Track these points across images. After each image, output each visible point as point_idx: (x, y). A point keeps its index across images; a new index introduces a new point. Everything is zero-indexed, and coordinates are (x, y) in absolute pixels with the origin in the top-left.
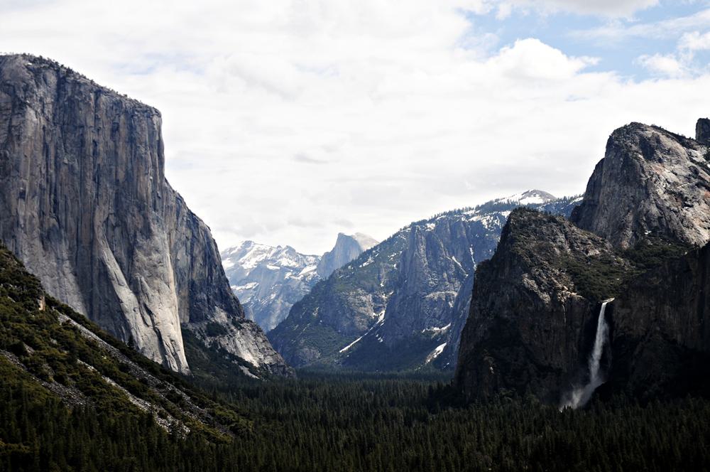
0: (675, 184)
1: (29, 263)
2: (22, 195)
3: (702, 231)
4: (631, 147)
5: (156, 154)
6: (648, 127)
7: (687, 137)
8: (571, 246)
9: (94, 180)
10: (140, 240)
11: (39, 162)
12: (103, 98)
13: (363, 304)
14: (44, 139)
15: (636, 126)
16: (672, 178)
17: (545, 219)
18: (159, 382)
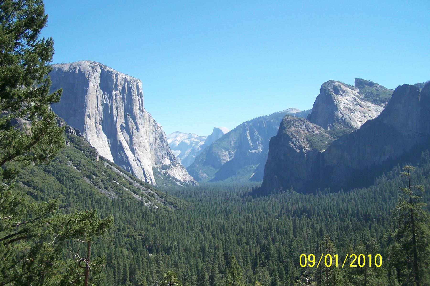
0: (347, 104)
1: (92, 143)
2: (89, 117)
3: (358, 123)
5: (140, 98)
7: (352, 85)
8: (308, 130)
10: (135, 132)
11: (95, 103)
12: (119, 76)
13: (225, 155)
14: (96, 94)
15: (332, 82)
16: (346, 102)
18: (145, 189)
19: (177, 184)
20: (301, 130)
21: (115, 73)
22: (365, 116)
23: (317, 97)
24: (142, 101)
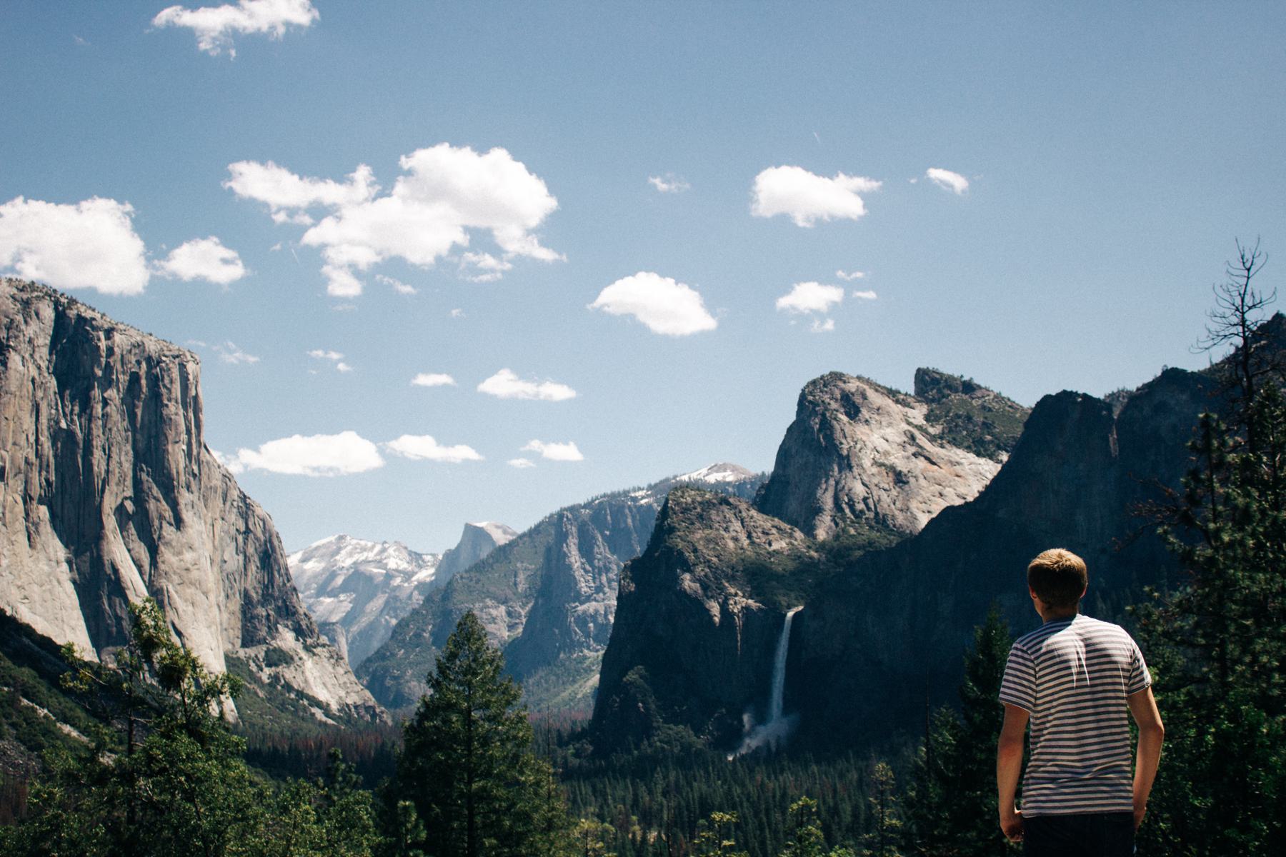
0: (886, 453)
1: (8, 566)
4: (829, 404)
5: (191, 415)
6: (852, 378)
7: (903, 391)
8: (749, 537)
9: (104, 450)
10: (169, 532)
11: (25, 427)
12: (117, 338)
13: (494, 620)
14: (34, 395)
15: (837, 376)
16: (882, 446)
17: (715, 501)
19: (313, 715)
20: (726, 535)
21: (106, 327)
22: (941, 495)
23: (790, 430)
24: (198, 427)
